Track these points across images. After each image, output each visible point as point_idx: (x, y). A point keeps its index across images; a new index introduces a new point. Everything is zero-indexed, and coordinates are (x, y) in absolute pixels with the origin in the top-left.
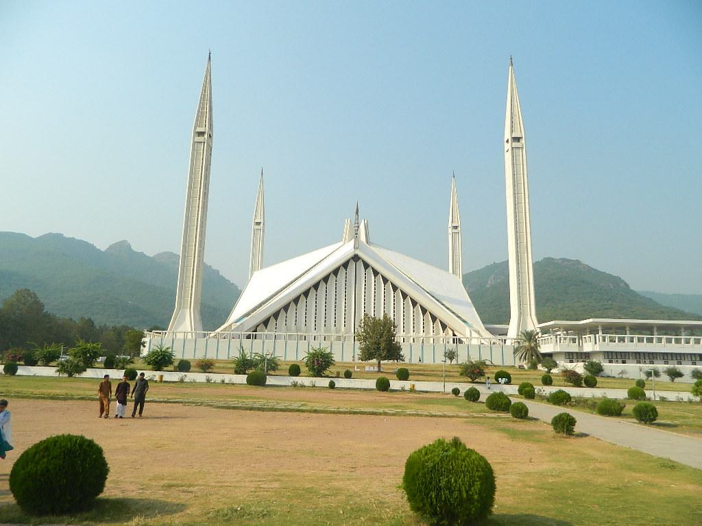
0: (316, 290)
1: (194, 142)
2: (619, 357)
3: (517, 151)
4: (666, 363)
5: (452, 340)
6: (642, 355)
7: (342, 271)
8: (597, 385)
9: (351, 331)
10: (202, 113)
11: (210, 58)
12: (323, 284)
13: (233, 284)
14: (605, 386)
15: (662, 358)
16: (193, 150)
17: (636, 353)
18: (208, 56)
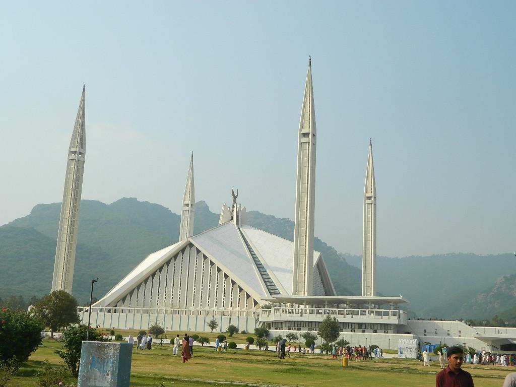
1: (69, 160)
2: (296, 325)
3: (305, 145)
7: (180, 255)
10: (76, 137)
11: (84, 91)
13: (330, 247)
17: (309, 322)
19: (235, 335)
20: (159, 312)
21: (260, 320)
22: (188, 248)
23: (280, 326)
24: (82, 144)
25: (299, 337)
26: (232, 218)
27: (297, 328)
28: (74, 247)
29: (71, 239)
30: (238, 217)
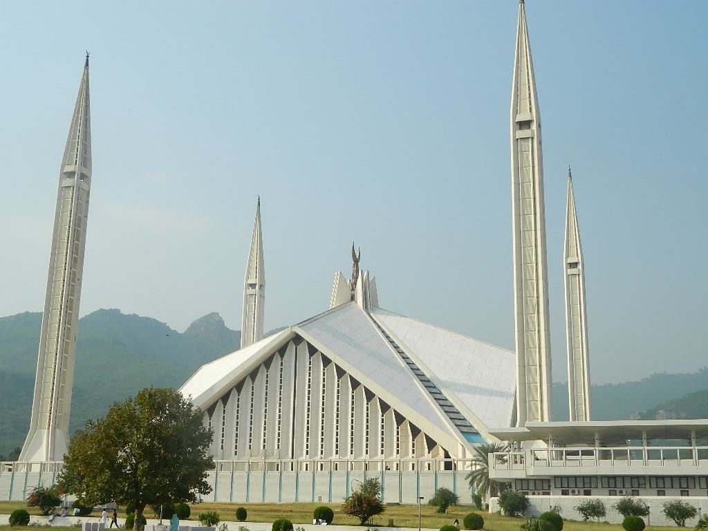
0: (239, 392)
1: (63, 189)
2: (580, 484)
4: (661, 493)
5: (442, 465)
6: (619, 482)
7: (277, 359)
8: (190, 517)
9: (288, 454)
11: (87, 64)
12: (248, 382)
14: (403, 524)
15: (654, 485)
16: (59, 199)
17: (609, 477)
18: (85, 64)
19: (450, 509)
20: (235, 467)
21: (493, 475)
22: (292, 347)
23: (532, 486)
24: (86, 161)
25: (608, 506)
26: (353, 298)
27: (582, 491)
28: (72, 347)
29: (67, 333)
30: (365, 294)
